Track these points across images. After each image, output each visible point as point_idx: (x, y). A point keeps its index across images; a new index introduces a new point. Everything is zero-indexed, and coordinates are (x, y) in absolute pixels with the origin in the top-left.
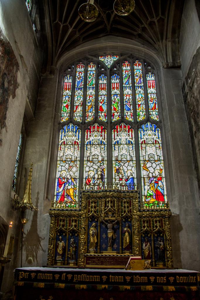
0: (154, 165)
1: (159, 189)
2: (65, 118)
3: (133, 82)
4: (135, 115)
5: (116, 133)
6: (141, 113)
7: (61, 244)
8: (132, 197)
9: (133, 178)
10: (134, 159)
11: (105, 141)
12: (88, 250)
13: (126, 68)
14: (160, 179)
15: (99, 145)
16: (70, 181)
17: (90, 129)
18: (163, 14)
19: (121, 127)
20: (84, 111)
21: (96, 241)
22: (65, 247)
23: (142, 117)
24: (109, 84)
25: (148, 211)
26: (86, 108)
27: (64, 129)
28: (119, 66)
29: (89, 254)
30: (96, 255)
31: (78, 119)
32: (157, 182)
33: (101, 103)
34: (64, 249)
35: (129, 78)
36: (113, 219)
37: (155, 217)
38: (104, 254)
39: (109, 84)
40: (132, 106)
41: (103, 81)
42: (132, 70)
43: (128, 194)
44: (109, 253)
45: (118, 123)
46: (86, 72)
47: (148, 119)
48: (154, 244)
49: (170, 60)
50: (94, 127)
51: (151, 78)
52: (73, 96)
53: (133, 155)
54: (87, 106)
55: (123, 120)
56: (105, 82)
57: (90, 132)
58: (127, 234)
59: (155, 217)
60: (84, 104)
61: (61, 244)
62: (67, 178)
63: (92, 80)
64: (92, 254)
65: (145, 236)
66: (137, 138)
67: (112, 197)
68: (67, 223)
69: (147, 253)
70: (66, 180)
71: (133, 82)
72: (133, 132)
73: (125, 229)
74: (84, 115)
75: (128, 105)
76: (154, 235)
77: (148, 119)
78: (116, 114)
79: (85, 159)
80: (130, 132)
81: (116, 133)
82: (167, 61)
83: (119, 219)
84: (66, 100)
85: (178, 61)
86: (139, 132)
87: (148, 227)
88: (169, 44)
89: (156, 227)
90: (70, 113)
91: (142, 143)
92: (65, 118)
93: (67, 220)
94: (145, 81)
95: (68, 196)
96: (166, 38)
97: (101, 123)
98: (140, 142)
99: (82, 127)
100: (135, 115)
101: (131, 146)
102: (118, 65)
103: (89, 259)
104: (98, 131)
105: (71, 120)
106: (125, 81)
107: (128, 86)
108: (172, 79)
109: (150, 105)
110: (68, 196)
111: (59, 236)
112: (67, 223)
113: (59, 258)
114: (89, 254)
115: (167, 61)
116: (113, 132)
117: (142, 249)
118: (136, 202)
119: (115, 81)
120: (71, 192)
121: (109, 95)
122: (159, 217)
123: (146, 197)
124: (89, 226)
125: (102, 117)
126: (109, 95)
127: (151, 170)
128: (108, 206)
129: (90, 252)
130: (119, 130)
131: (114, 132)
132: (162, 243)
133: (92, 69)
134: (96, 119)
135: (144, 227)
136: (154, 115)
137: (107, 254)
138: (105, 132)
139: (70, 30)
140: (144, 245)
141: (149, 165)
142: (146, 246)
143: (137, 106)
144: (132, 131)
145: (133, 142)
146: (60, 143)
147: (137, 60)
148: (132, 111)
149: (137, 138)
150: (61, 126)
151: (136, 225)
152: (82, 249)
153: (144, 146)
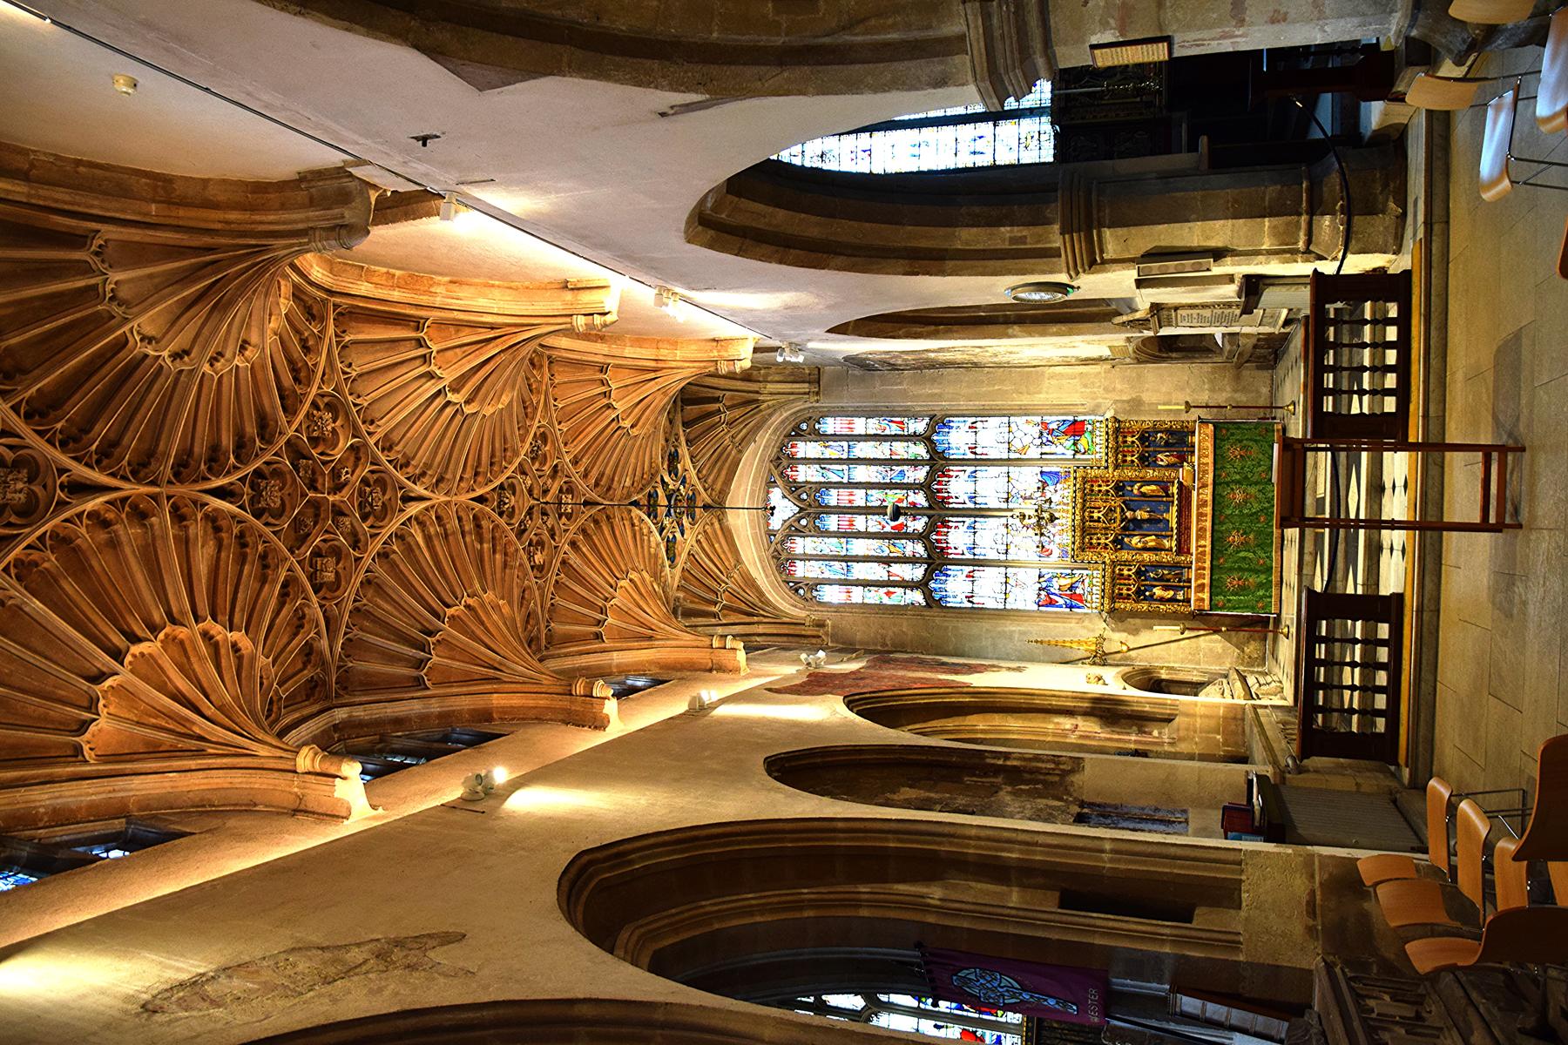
0: (1019, 434)
1: (1062, 428)
2: (917, 597)
3: (839, 461)
4: (914, 463)
5: (951, 501)
6: (910, 451)
7: (1158, 592)
8: (1084, 478)
9: (1041, 472)
10: (1005, 469)
11: (969, 521)
12: (1167, 550)
13: (804, 474)
14: (1045, 425)
15: (975, 533)
16: (1044, 585)
17: (942, 549)
18: (717, 400)
19: (939, 491)
20: (903, 560)
21: (1153, 537)
22: (1163, 586)
23: (920, 450)
24: (839, 510)
25: (1107, 454)
26: (895, 557)
27: (941, 599)
28: (796, 489)
29: (1174, 549)
30: (1175, 537)
31: (918, 573)
32: (1051, 432)
33: (883, 527)
34: (1166, 588)
35: (829, 470)
36: (1118, 510)
37: (1117, 443)
38: (1175, 526)
39: (839, 510)
40: (894, 468)
41: (832, 522)
42: (807, 461)
43: (1078, 486)
44: (1172, 516)
45: (931, 495)
46: (806, 558)
47: (926, 439)
48: (1160, 446)
49: (805, 387)
50: (938, 541)
51: (830, 425)
52: (866, 584)
53: (994, 471)
54: (891, 555)
55: (925, 487)
56: (834, 518)
57: (948, 548)
58: (1142, 490)
59: (1117, 443)
60: (887, 561)
61: (1158, 592)
62: (1040, 589)
63: (830, 546)
64: (1174, 543)
65: (1146, 461)
66: (962, 462)
67: (1083, 509)
68: (1125, 584)
69: (1173, 460)
70: (1042, 592)
71: (839, 461)
72: (951, 468)
73: (1135, 492)
74: (913, 560)
75: (893, 475)
76: (1146, 447)
77: (926, 439)
78: (910, 500)
79: (1003, 557)
80: (951, 473)
81: (951, 501)
82: (808, 393)
83: (1119, 501)
84: (875, 596)
85: (807, 371)
86: (951, 457)
87: (1133, 456)
88: (771, 387)
89: (1133, 442)
90: (905, 587)
91: (975, 453)
92: (917, 597)
93: (1121, 584)
94: (836, 437)
95: (1071, 587)
96: (757, 392)
97: (931, 527)
98: (973, 456)
99: (939, 565)
100: (914, 463)
101: (978, 474)
102: (794, 489)
103: (1183, 548)
104: (946, 534)
105: (922, 585)
106: (834, 478)
107: (846, 472)
108: (845, 388)
109: (893, 433)
110: (1072, 588)
111: (1145, 596)
112: (1125, 584)
113: (1180, 596)
114: (1174, 549)
115: (808, 393)
116: (951, 506)
117: (1168, 466)
118: (1093, 473)
119: (832, 498)
120: (1063, 582)
121: (867, 511)
122: (1117, 437)
123: (1076, 452)
124: (1130, 548)
125: (919, 525)
126: (867, 511)
127: (1027, 440)
128: (1099, 518)
129: (1171, 548)
130: (946, 495)
131: (949, 503)
132: (1159, 435)
133: (801, 545)
134: (922, 537)
135: (1133, 461)
136: (919, 426)
137: (1175, 520)
138: (949, 521)
139: (731, 585)
140: (1161, 463)
141: (1017, 444)
142: (1162, 460)
143: (893, 457)
144: (949, 470)
145: (973, 469)
146: (970, 605)
147: (781, 450)
148: (905, 468)
149: (962, 462)
150: (934, 602)
151: (1130, 473)
152: (1166, 558)
153: (978, 451)
